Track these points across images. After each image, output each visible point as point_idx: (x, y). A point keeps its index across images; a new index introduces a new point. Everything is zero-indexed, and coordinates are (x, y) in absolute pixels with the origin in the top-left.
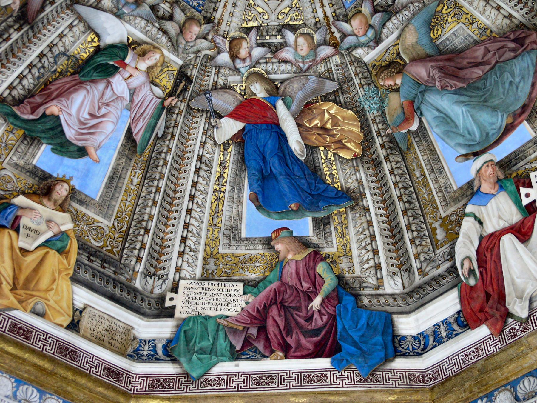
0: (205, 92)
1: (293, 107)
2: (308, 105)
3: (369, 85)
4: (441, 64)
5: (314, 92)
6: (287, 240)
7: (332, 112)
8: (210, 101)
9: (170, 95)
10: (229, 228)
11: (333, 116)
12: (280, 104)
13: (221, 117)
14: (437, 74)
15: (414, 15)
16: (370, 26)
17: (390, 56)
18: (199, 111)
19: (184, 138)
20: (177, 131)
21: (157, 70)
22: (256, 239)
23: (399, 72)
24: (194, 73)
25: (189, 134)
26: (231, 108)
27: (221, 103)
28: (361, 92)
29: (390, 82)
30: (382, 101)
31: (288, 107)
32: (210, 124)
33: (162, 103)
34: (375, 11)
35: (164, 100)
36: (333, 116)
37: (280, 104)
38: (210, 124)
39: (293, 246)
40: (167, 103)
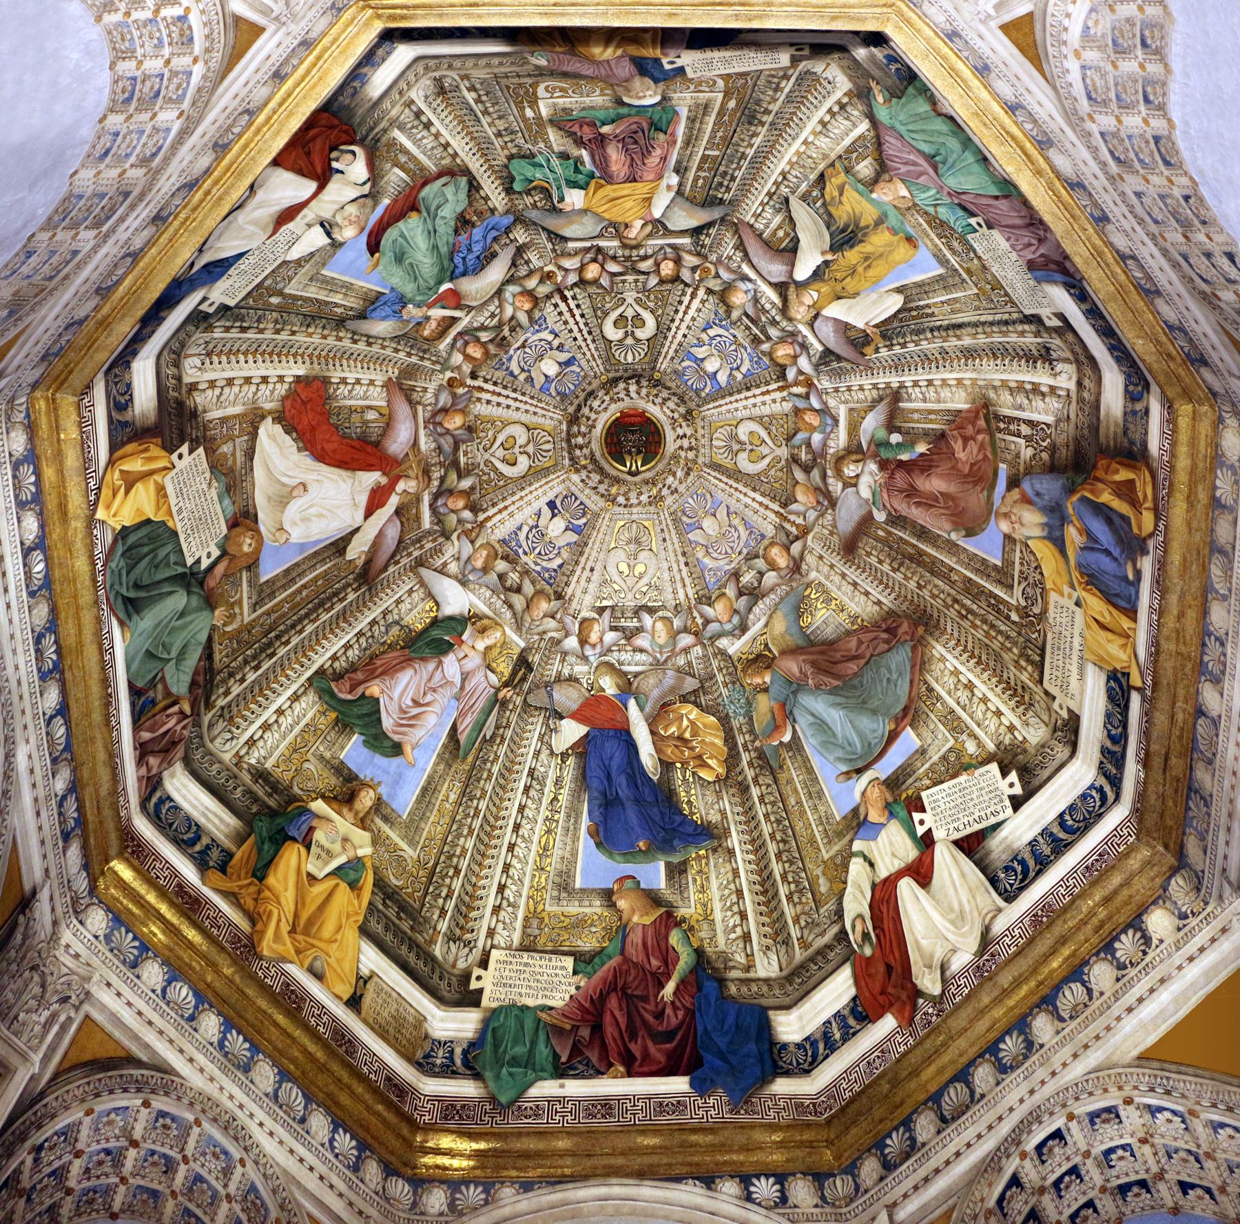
0: (547, 685)
1: (648, 709)
2: (664, 705)
3: (734, 683)
4: (814, 657)
5: (672, 690)
6: (633, 895)
7: (692, 717)
8: (550, 696)
9: (506, 685)
10: (560, 874)
11: (692, 722)
12: (632, 703)
13: (561, 718)
14: (809, 670)
15: (782, 599)
16: (736, 611)
17: (758, 648)
18: (536, 708)
19: (515, 743)
20: (509, 733)
21: (496, 652)
22: (594, 890)
23: (768, 667)
24: (535, 659)
25: (522, 739)
26: (575, 707)
27: (563, 699)
28: (725, 692)
29: (758, 680)
30: (749, 703)
31: (642, 709)
32: (548, 726)
33: (496, 694)
34: (741, 594)
35: (498, 690)
36: (692, 722)
37: (632, 703)
38: (548, 726)
39: (640, 903)
40: (501, 695)
